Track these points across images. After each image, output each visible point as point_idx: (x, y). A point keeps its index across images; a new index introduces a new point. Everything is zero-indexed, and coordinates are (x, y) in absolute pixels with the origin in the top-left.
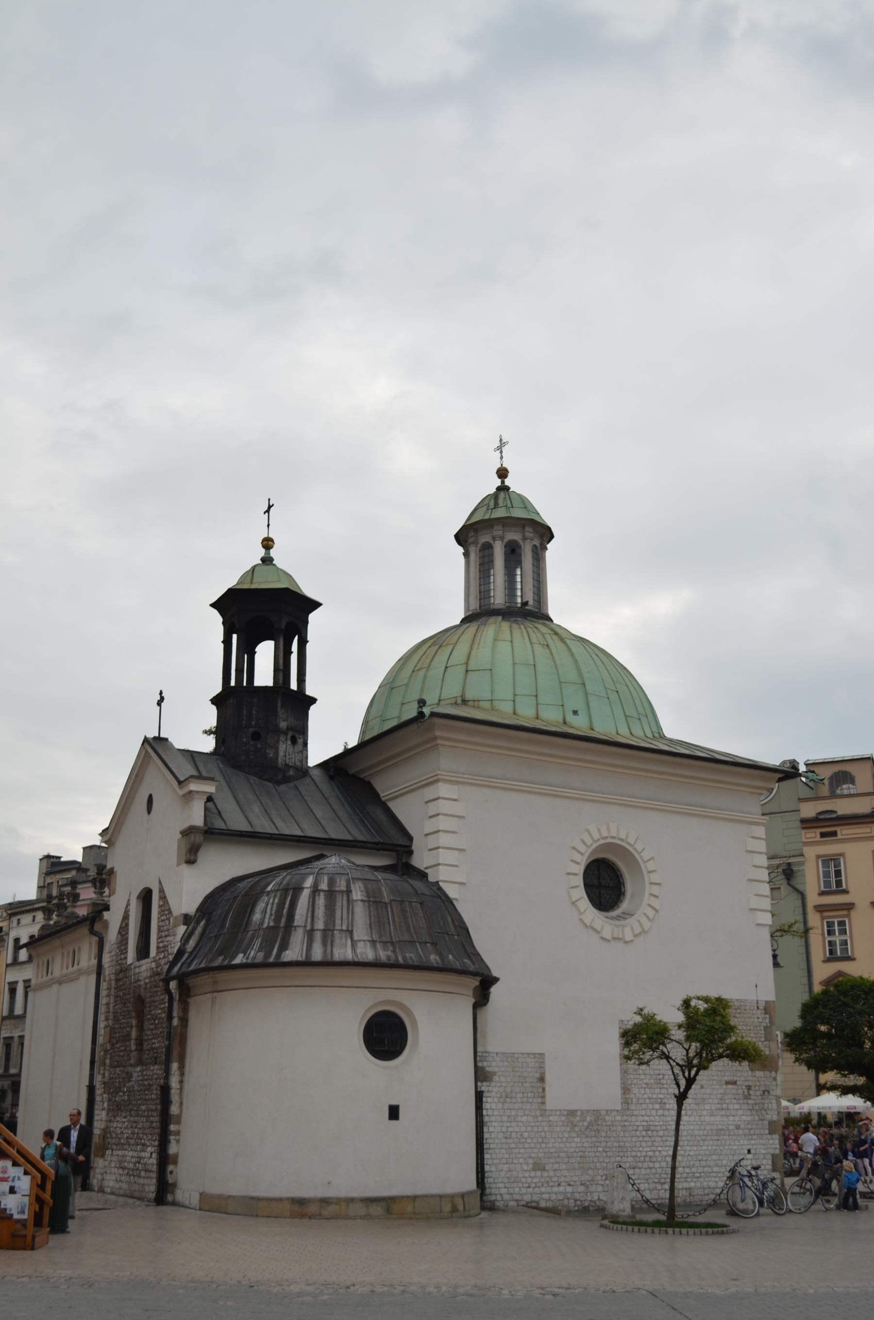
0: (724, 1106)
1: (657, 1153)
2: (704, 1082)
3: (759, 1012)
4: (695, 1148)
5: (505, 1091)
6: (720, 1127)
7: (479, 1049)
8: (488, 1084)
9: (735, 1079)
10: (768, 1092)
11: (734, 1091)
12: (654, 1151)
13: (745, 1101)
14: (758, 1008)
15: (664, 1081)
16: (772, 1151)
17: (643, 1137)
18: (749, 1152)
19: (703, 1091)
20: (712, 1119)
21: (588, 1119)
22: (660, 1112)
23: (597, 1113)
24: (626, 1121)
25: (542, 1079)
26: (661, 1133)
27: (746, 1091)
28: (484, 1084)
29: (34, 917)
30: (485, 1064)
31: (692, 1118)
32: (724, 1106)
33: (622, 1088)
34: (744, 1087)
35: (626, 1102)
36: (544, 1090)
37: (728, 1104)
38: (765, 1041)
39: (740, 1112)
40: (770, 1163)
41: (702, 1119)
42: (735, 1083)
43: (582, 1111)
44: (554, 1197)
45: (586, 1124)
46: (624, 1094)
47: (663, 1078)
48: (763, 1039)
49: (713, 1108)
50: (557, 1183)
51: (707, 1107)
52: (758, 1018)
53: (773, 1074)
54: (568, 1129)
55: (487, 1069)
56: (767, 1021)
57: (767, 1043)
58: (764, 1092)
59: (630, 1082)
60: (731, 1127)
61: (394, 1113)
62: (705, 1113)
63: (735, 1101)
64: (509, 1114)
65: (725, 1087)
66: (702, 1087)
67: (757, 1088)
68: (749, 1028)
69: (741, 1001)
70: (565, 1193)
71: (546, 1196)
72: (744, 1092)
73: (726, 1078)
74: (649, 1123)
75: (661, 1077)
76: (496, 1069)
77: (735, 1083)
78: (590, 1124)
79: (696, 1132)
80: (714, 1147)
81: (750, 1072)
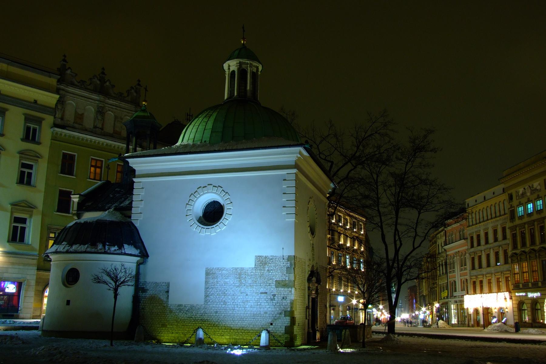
0: (259, 304)
1: (220, 323)
2: (248, 293)
3: (284, 261)
4: (241, 322)
5: (152, 296)
6: (255, 313)
7: (141, 280)
8: (145, 294)
9: (267, 291)
10: (286, 297)
11: (266, 297)
12: (219, 322)
13: (271, 302)
14: (283, 259)
15: (227, 293)
16: (286, 325)
17: (214, 316)
18: (272, 324)
19: (247, 297)
20: (251, 309)
21: (188, 308)
22: (224, 306)
23: (192, 307)
24: (206, 309)
25: (168, 292)
26: (223, 315)
27: (272, 297)
28: (144, 294)
29: (441, 235)
30: (144, 286)
31: (240, 309)
32: (259, 304)
33: (205, 296)
34: (271, 295)
35: (206, 301)
36: (168, 296)
37: (261, 303)
38: (287, 274)
39: (268, 306)
40: (284, 329)
41: (246, 309)
42: (266, 293)
43: (185, 305)
44: (169, 338)
45: (186, 309)
46: (206, 298)
47: (226, 291)
48: (285, 273)
49: (252, 304)
50: (171, 333)
51: (250, 304)
52: (283, 263)
53: (290, 289)
54: (178, 311)
55: (145, 288)
56: (289, 265)
57: (287, 275)
58: (283, 298)
59: (209, 293)
60: (262, 313)
61: (68, 303)
62: (247, 306)
63: (265, 301)
64: (153, 305)
65: (260, 295)
66: (247, 295)
67: (279, 295)
68: (277, 268)
69: (273, 256)
70: (174, 337)
71: (166, 338)
72: (271, 297)
73: (261, 291)
74: (217, 310)
75: (225, 291)
76: (148, 288)
77: (266, 293)
78: (189, 309)
79: (242, 315)
80: (251, 322)
81: (276, 289)
